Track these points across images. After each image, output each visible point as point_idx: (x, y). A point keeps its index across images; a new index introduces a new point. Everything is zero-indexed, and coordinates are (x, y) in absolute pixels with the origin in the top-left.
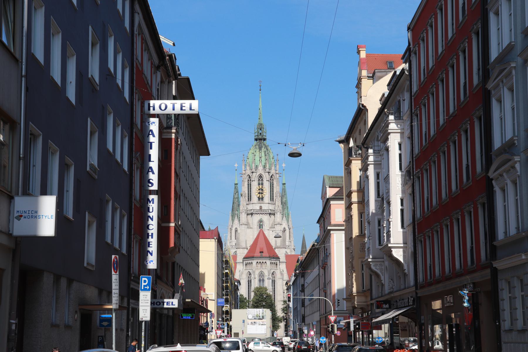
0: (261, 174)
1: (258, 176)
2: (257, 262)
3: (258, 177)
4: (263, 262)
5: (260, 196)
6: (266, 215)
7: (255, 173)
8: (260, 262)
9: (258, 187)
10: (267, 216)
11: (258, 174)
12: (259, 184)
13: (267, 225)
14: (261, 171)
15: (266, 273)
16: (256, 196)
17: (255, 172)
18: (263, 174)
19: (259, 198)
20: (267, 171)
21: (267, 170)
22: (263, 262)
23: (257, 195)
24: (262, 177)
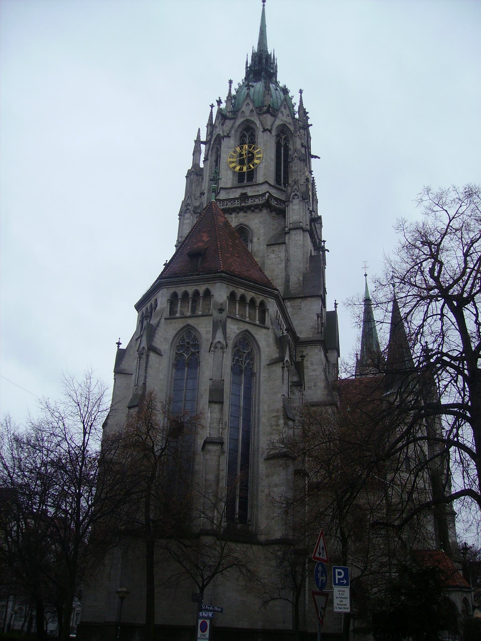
0: (247, 121)
1: (239, 126)
2: (175, 295)
3: (240, 130)
4: (196, 293)
5: (241, 169)
6: (256, 213)
7: (232, 121)
8: (186, 294)
9: (238, 149)
10: (260, 215)
11: (239, 121)
12: (242, 143)
13: (258, 239)
14: (247, 113)
15: (207, 332)
16: (230, 173)
17: (233, 117)
18: (255, 119)
19: (241, 176)
20: (264, 111)
21: (265, 109)
22: (196, 293)
23: (234, 168)
24: (252, 129)
